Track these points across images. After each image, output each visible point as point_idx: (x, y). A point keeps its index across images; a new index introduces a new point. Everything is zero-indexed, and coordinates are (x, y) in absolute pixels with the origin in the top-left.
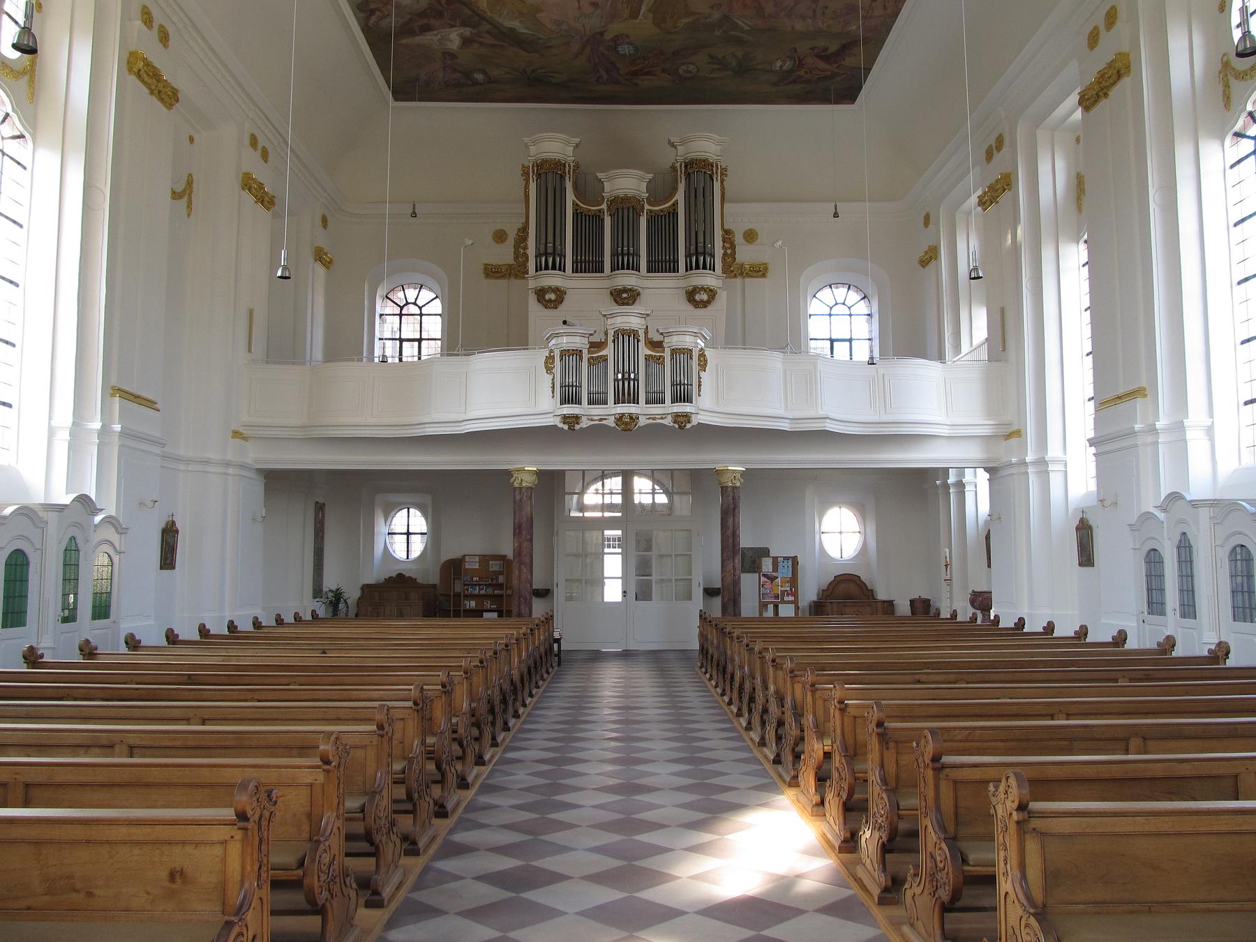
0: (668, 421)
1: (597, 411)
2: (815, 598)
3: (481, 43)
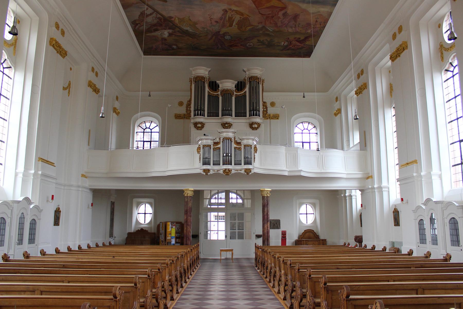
1: (216, 167)
2: (297, 238)
3: (175, 35)
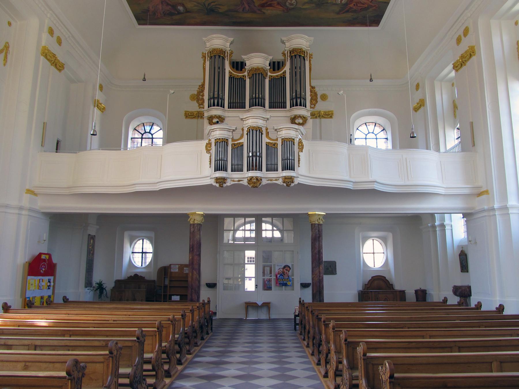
0: (280, 182)
1: (237, 175)
2: (361, 289)
